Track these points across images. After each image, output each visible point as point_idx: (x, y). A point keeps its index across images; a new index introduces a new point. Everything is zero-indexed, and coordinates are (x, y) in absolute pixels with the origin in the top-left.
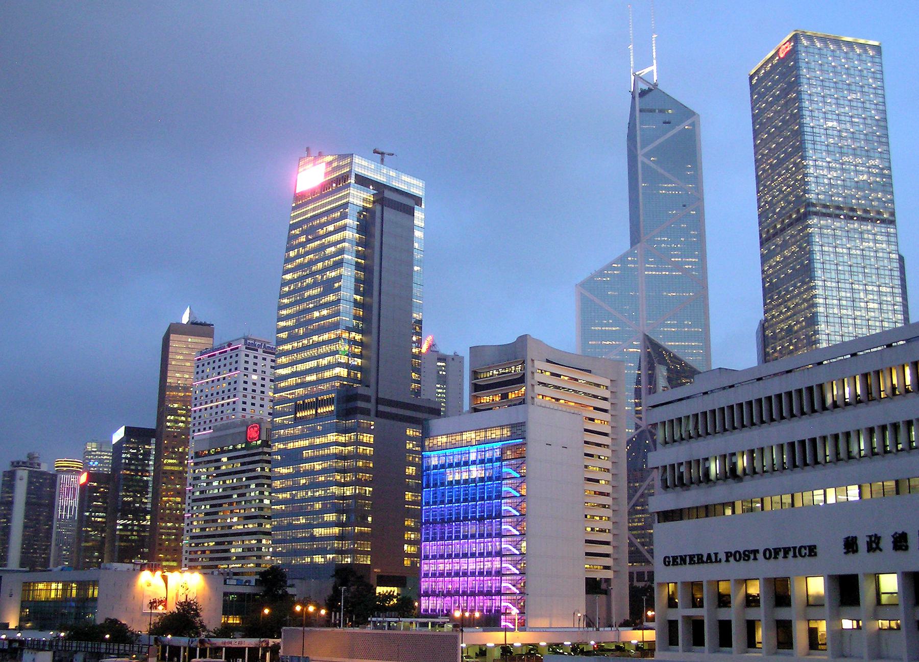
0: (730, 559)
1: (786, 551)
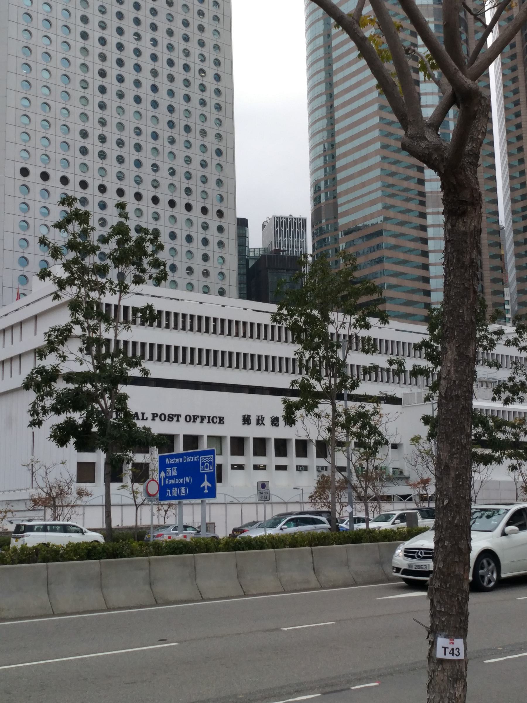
0: (155, 418)
1: (203, 418)
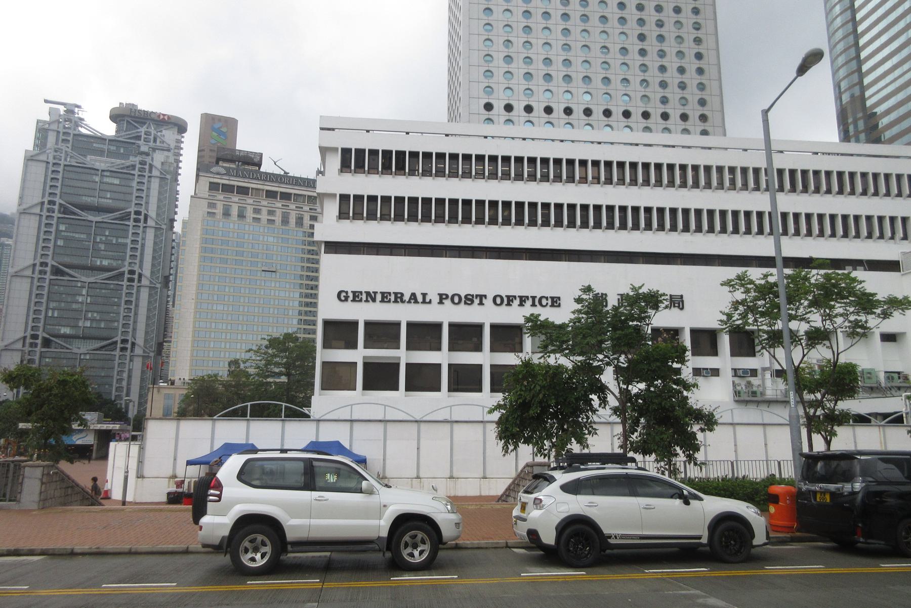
0: (444, 301)
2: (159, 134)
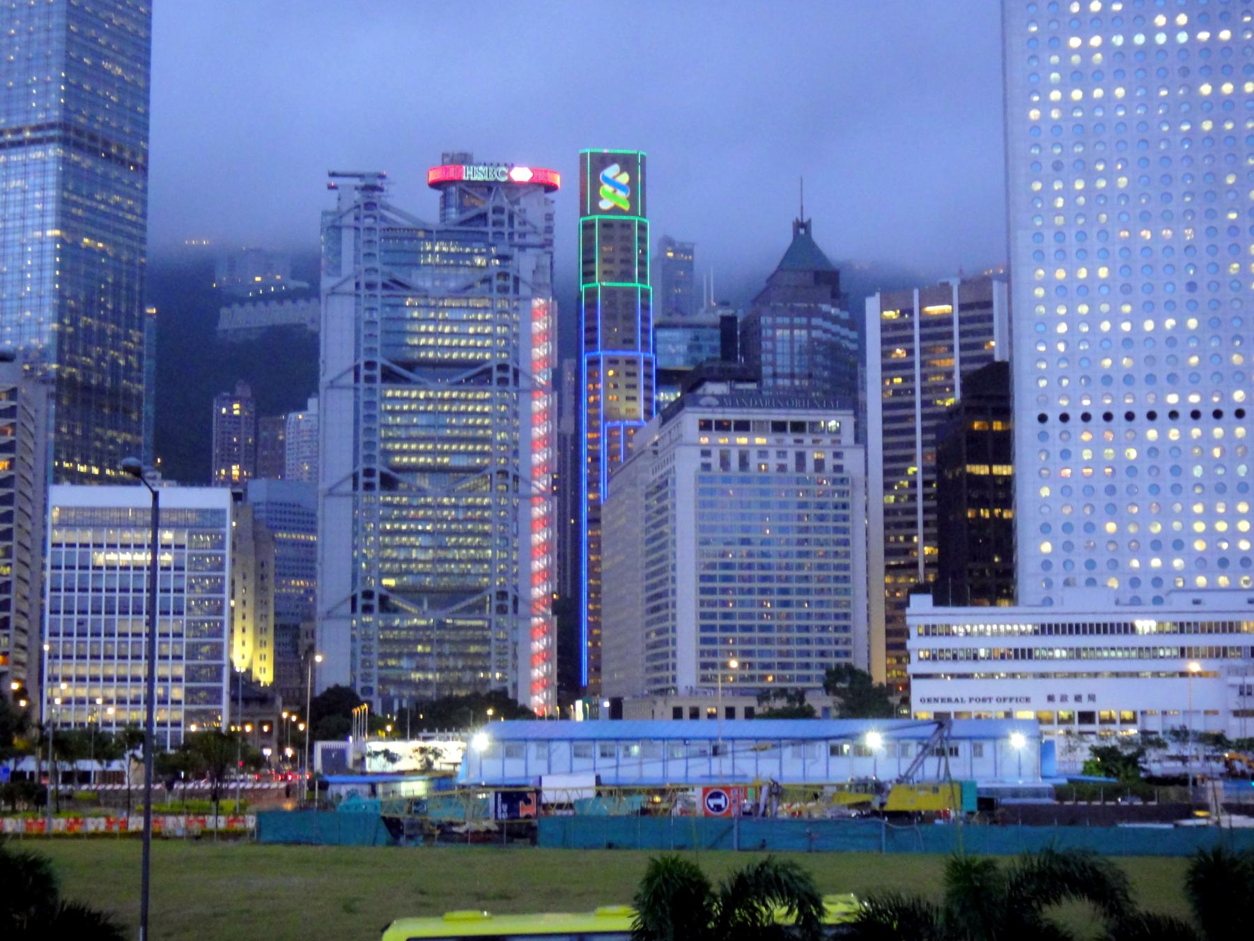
1: (1011, 700)
2: (516, 208)
